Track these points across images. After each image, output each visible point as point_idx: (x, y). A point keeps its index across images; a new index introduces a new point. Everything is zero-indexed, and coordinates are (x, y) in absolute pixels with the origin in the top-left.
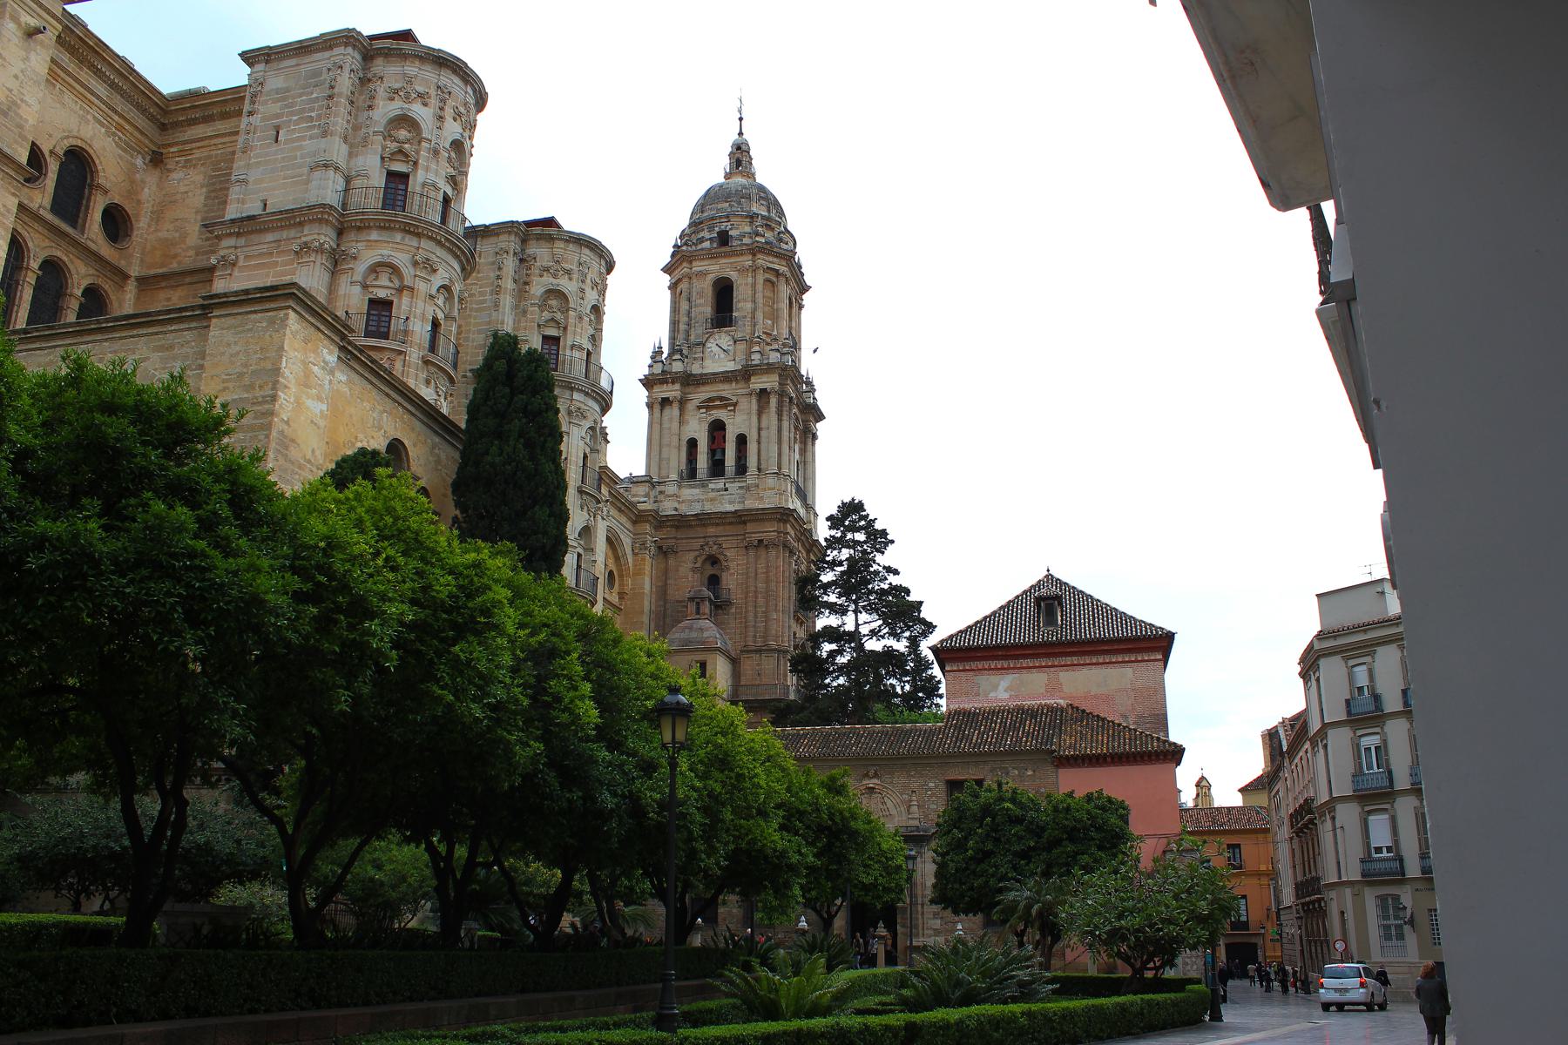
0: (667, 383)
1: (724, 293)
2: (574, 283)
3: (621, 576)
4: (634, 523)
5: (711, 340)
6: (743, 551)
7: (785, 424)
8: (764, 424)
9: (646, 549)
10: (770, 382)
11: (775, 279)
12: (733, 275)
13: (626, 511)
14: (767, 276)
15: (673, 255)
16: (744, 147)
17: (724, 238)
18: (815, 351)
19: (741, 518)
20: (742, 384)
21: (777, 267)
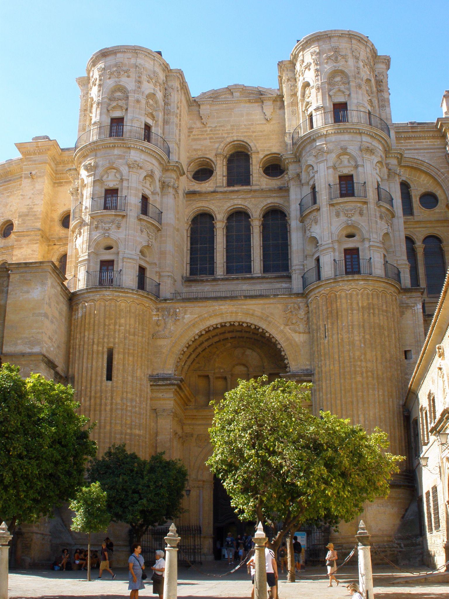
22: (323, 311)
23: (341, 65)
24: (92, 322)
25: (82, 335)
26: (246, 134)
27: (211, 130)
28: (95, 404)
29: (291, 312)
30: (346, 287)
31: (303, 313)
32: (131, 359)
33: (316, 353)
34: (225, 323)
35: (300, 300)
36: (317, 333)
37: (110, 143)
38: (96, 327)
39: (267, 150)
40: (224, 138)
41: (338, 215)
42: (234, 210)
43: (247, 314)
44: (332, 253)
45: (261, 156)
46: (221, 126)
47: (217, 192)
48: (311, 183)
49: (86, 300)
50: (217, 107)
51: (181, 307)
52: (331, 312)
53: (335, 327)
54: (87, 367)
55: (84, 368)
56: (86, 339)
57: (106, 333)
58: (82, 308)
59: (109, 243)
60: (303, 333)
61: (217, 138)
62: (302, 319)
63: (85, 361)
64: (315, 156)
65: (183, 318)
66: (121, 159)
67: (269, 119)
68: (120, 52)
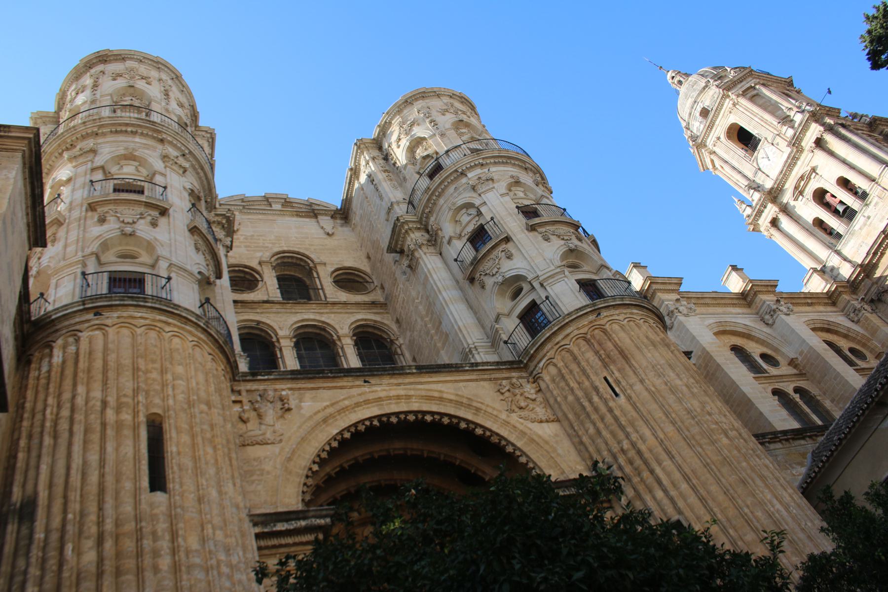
0: (762, 211)
3: (864, 345)
4: (834, 304)
5: (759, 161)
9: (859, 311)
11: (755, 92)
12: (733, 119)
13: (814, 301)
14: (748, 96)
16: (673, 75)
17: (705, 113)
18: (830, 92)
21: (748, 85)
22: (587, 361)
23: (464, 117)
24: (98, 364)
25: (67, 396)
26: (299, 246)
27: (246, 239)
28: (118, 555)
29: (509, 390)
30: (617, 318)
31: (533, 391)
32: (210, 450)
33: (604, 433)
34: (388, 415)
35: (514, 374)
36: (590, 401)
37: (127, 125)
38: (111, 375)
39: (337, 264)
40: (267, 247)
41: (547, 239)
42: (301, 331)
43: (430, 398)
44: (566, 279)
45: (330, 269)
46: (261, 236)
47: (273, 302)
48: (470, 228)
49: (77, 327)
50: (250, 217)
51: (291, 389)
52: (608, 356)
53: (631, 373)
54: (85, 463)
55: (74, 466)
56: (80, 401)
57: (142, 385)
58: (64, 347)
59: (131, 248)
60: (547, 421)
61: (257, 247)
62: (534, 400)
63: (77, 448)
64: (474, 188)
65: (300, 408)
66: (148, 149)
67: (330, 233)
68: (131, 59)
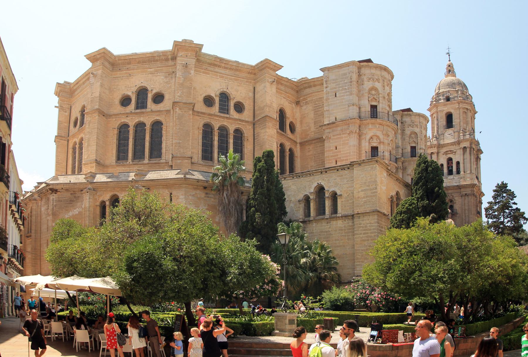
1: (449, 118)
2: (419, 129)
5: (446, 133)
6: (460, 197)
7: (472, 157)
8: (465, 157)
10: (467, 144)
15: (431, 105)
19: (459, 187)
20: (457, 146)
